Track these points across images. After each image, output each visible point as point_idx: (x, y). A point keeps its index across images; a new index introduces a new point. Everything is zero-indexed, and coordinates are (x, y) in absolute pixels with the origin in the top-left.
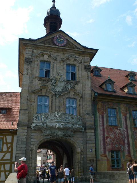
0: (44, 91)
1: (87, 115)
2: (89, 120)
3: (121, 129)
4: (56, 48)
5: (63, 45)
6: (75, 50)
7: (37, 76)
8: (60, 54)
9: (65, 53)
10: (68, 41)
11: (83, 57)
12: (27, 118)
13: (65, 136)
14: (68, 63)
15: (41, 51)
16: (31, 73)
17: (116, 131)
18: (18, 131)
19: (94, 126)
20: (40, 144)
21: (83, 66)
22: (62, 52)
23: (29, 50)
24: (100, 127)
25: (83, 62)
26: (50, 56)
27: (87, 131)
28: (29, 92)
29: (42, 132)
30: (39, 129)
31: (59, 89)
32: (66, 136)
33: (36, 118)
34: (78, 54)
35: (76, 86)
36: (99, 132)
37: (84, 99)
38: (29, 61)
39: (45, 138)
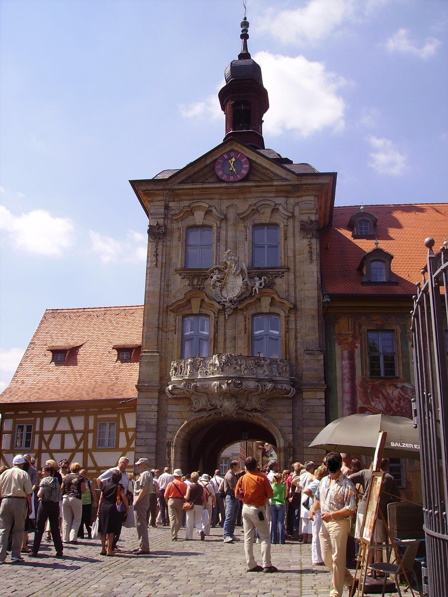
1: (307, 354)
2: (311, 367)
3: (407, 385)
4: (221, 188)
6: (273, 186)
8: (235, 202)
9: (248, 195)
10: (255, 162)
11: (297, 200)
12: (157, 370)
13: (248, 410)
14: (257, 222)
15: (186, 203)
16: (164, 261)
17: (390, 392)
18: (139, 402)
19: (323, 382)
20: (187, 430)
22: (240, 196)
23: (158, 203)
24: (343, 383)
25: (297, 213)
26: (208, 212)
27: (305, 395)
28: (161, 310)
29: (190, 404)
33: (176, 369)
34: (284, 194)
35: (278, 281)
36: (339, 395)
37: (299, 313)
38: (159, 234)
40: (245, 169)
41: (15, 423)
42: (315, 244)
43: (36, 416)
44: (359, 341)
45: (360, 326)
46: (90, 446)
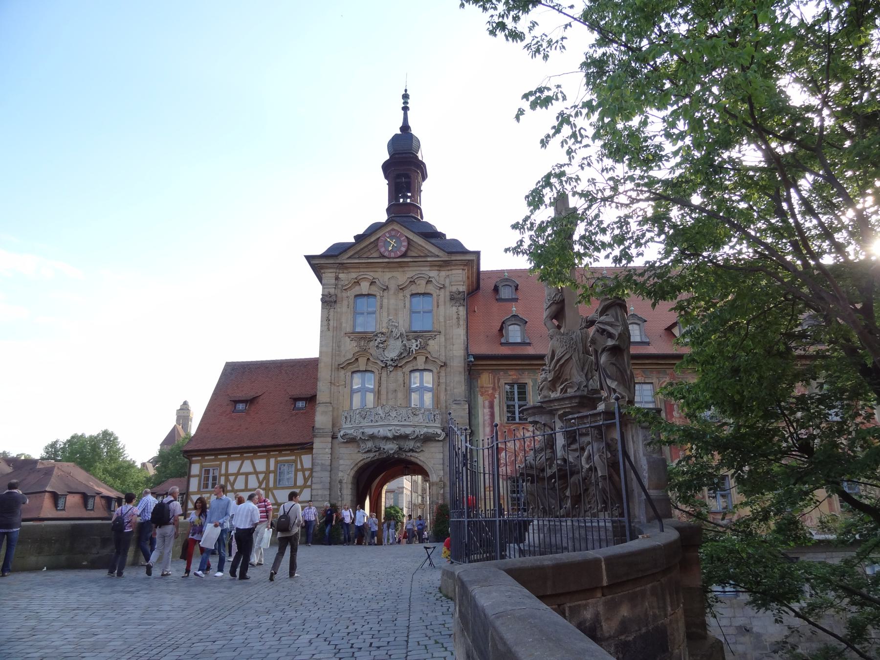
0: (362, 361)
2: (460, 414)
5: (399, 254)
7: (349, 330)
9: (406, 269)
13: (405, 451)
14: (414, 292)
20: (356, 469)
21: (448, 294)
22: (400, 269)
23: (330, 275)
25: (447, 284)
26: (372, 283)
30: (351, 441)
31: (392, 353)
32: (405, 451)
35: (431, 342)
39: (365, 456)
40: (404, 246)
41: (202, 467)
42: (462, 311)
43: (221, 460)
44: (497, 393)
45: (499, 380)
46: (271, 485)
